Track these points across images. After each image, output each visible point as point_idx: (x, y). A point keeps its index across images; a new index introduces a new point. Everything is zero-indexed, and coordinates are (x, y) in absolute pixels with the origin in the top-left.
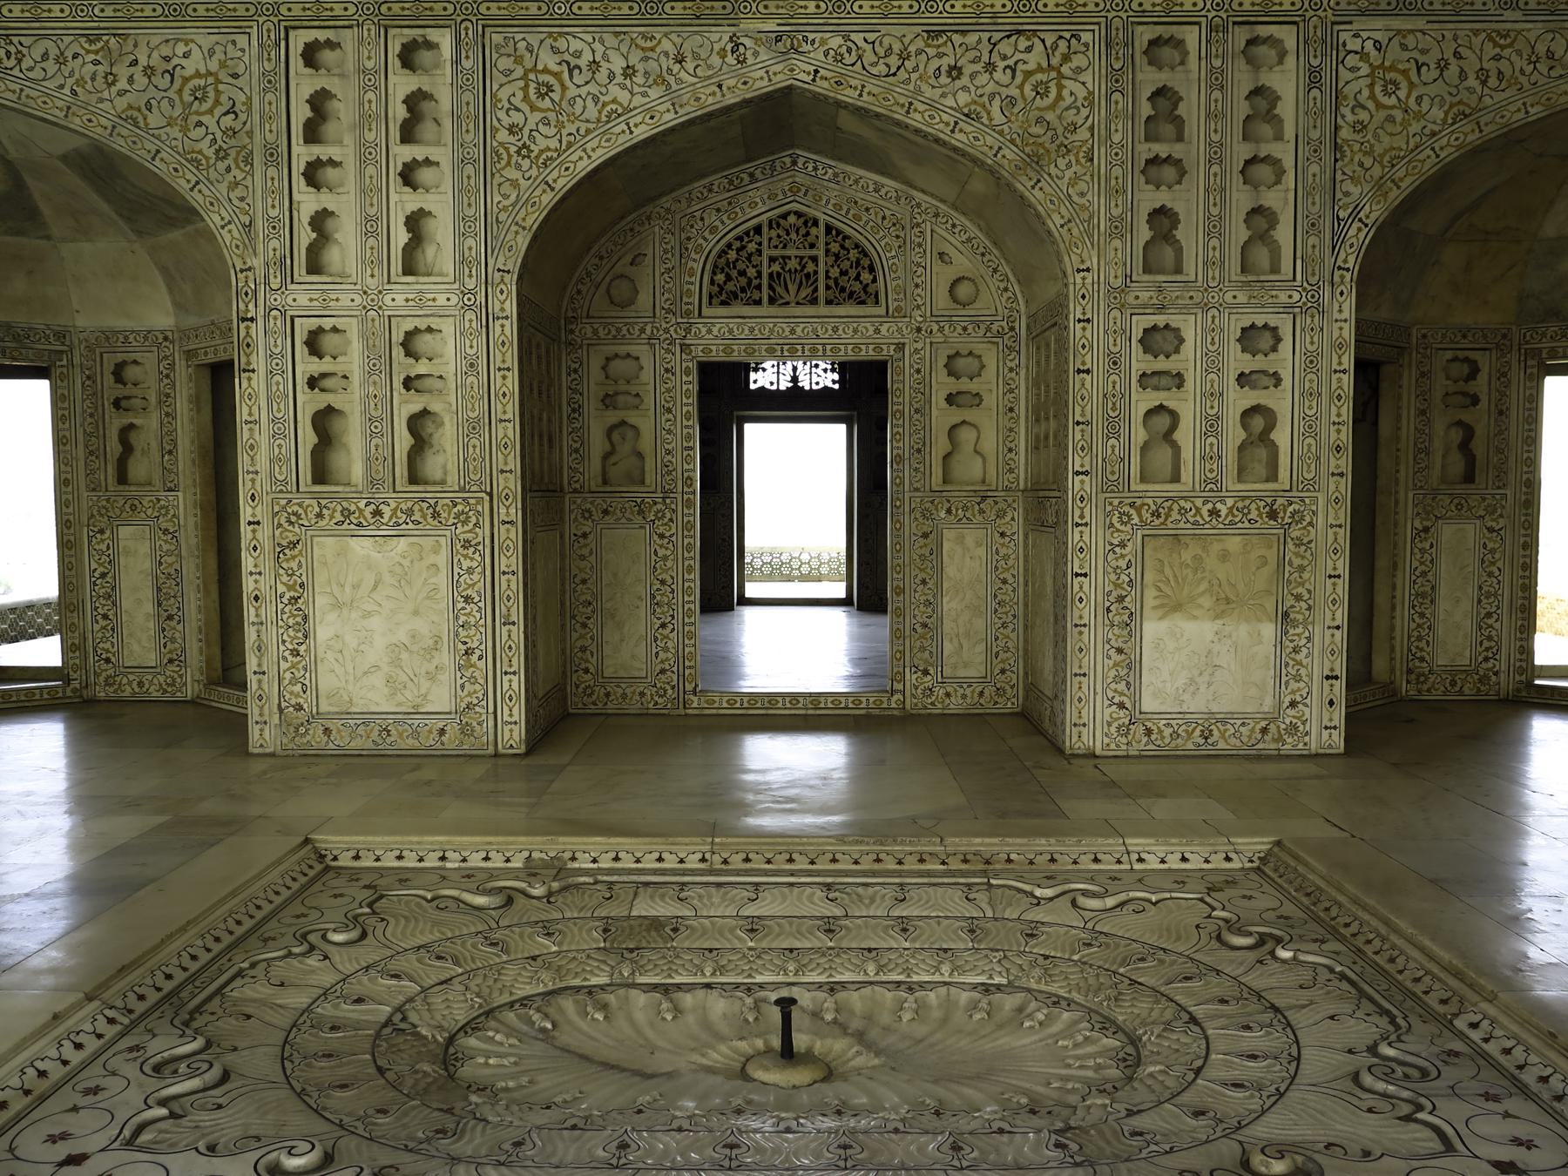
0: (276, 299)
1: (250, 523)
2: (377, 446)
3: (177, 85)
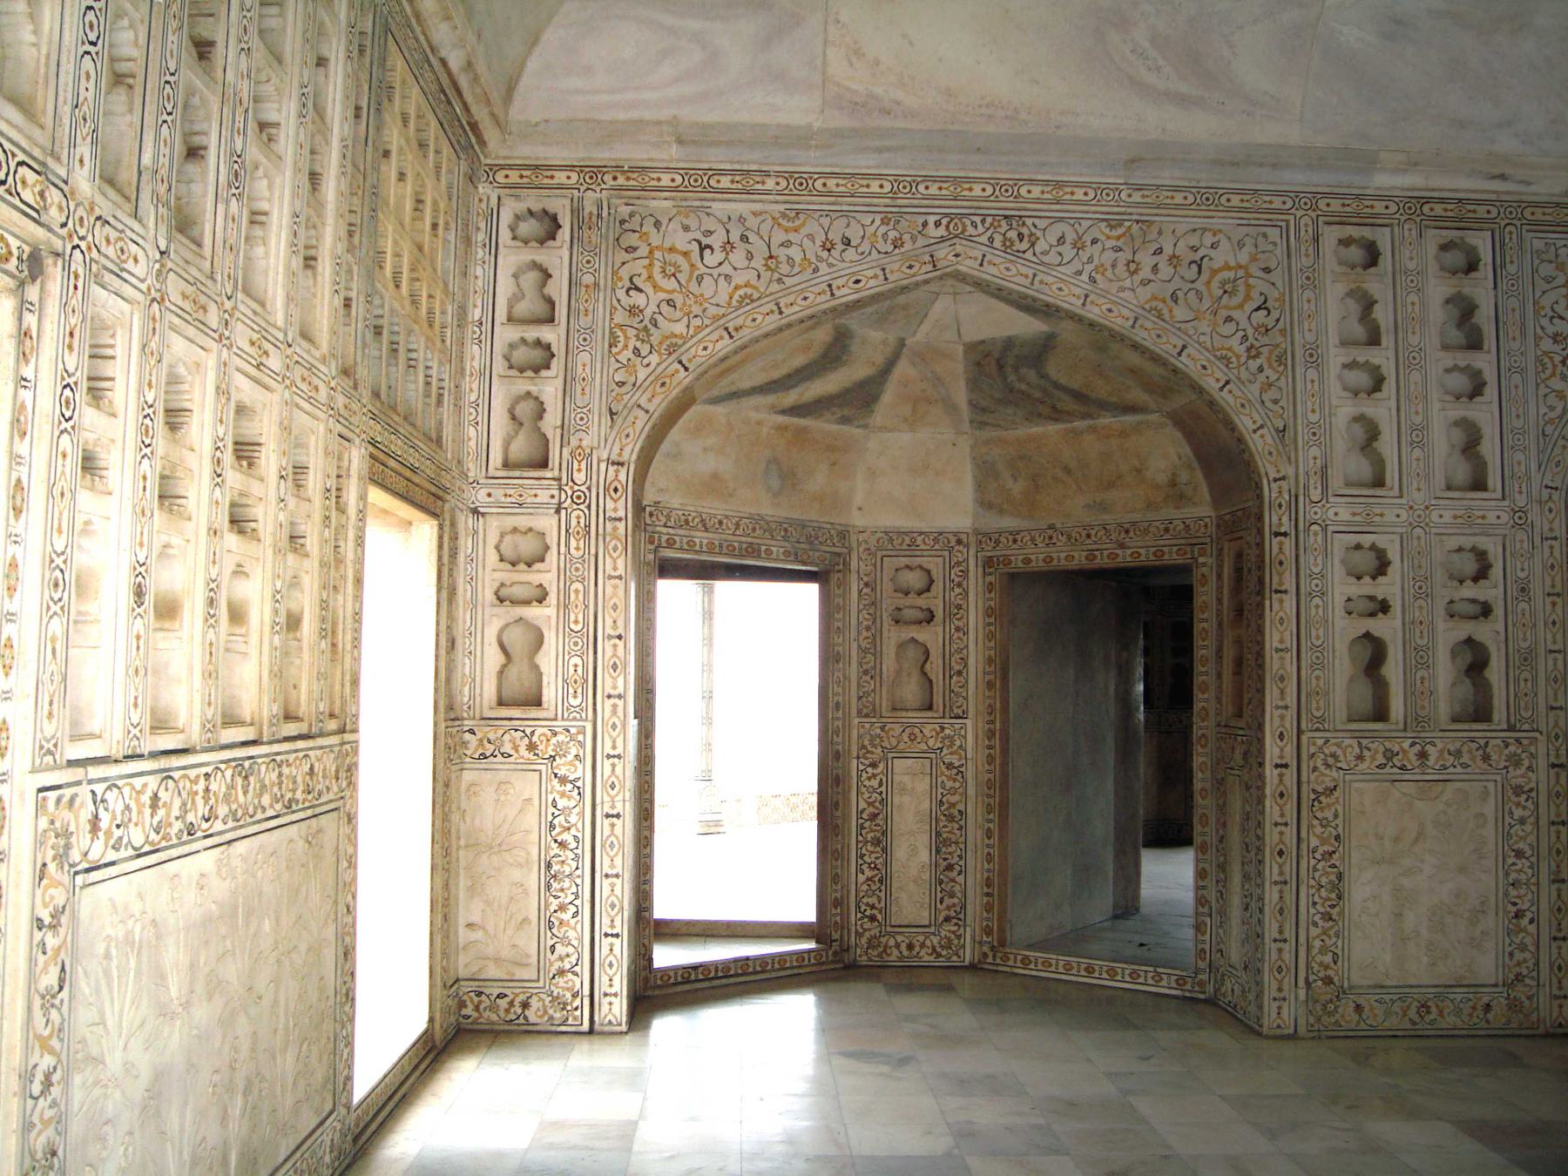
0: (1315, 513)
1: (1277, 766)
2: (1422, 679)
3: (1205, 276)
